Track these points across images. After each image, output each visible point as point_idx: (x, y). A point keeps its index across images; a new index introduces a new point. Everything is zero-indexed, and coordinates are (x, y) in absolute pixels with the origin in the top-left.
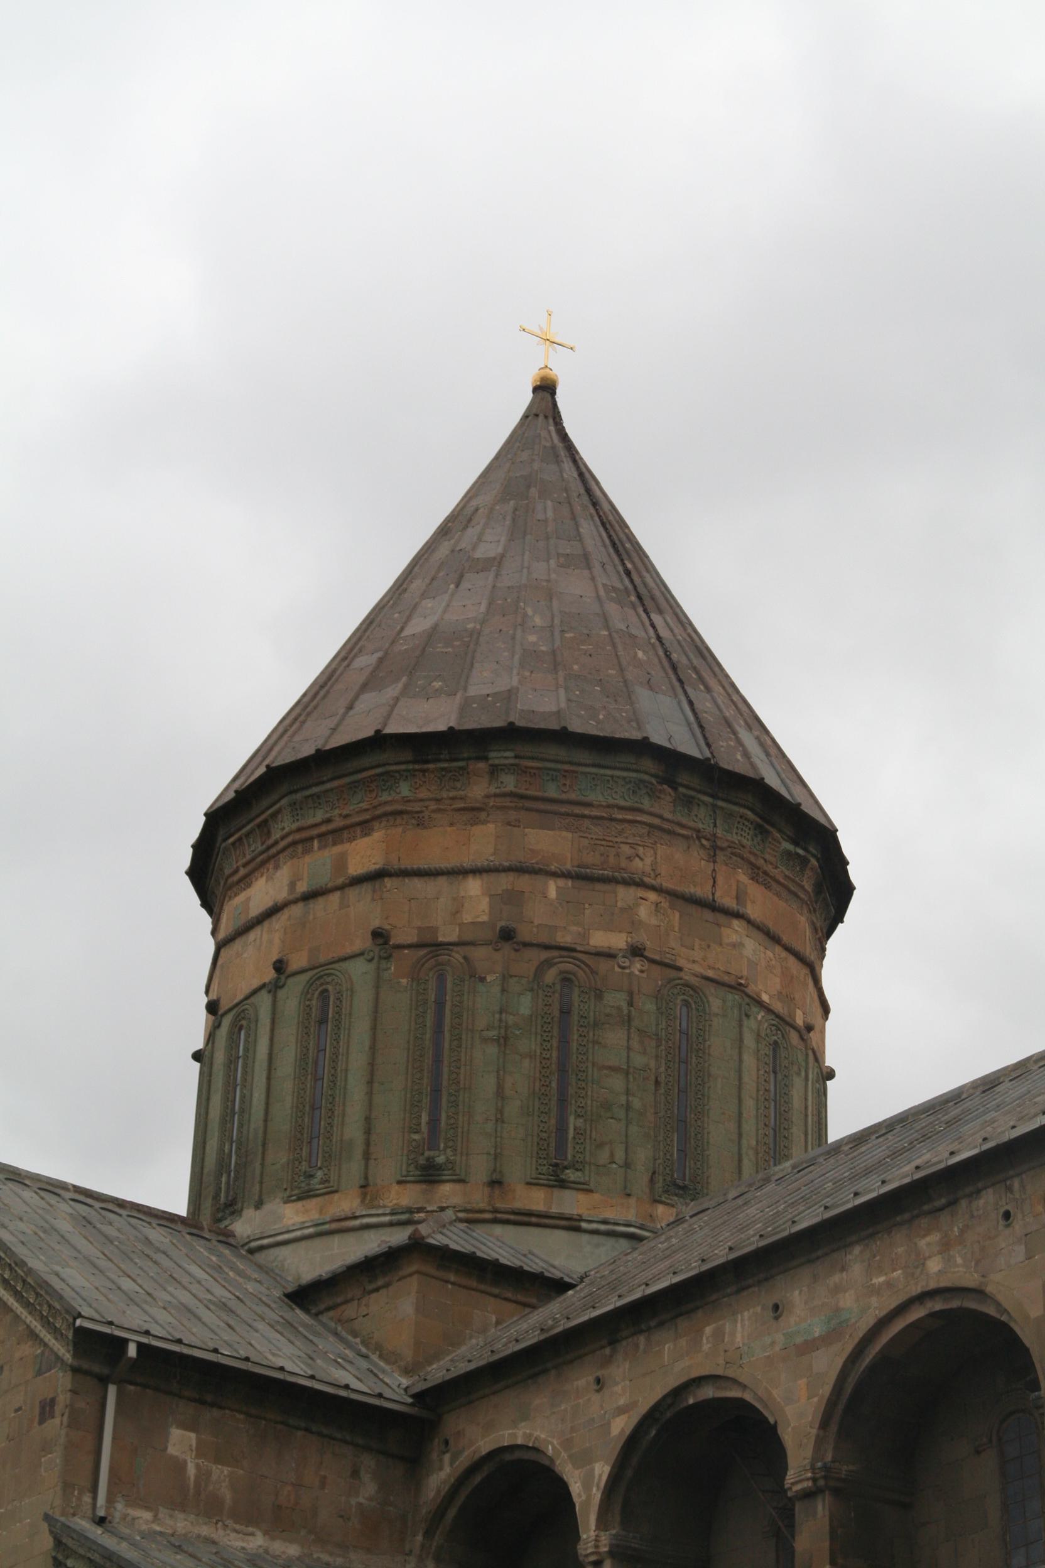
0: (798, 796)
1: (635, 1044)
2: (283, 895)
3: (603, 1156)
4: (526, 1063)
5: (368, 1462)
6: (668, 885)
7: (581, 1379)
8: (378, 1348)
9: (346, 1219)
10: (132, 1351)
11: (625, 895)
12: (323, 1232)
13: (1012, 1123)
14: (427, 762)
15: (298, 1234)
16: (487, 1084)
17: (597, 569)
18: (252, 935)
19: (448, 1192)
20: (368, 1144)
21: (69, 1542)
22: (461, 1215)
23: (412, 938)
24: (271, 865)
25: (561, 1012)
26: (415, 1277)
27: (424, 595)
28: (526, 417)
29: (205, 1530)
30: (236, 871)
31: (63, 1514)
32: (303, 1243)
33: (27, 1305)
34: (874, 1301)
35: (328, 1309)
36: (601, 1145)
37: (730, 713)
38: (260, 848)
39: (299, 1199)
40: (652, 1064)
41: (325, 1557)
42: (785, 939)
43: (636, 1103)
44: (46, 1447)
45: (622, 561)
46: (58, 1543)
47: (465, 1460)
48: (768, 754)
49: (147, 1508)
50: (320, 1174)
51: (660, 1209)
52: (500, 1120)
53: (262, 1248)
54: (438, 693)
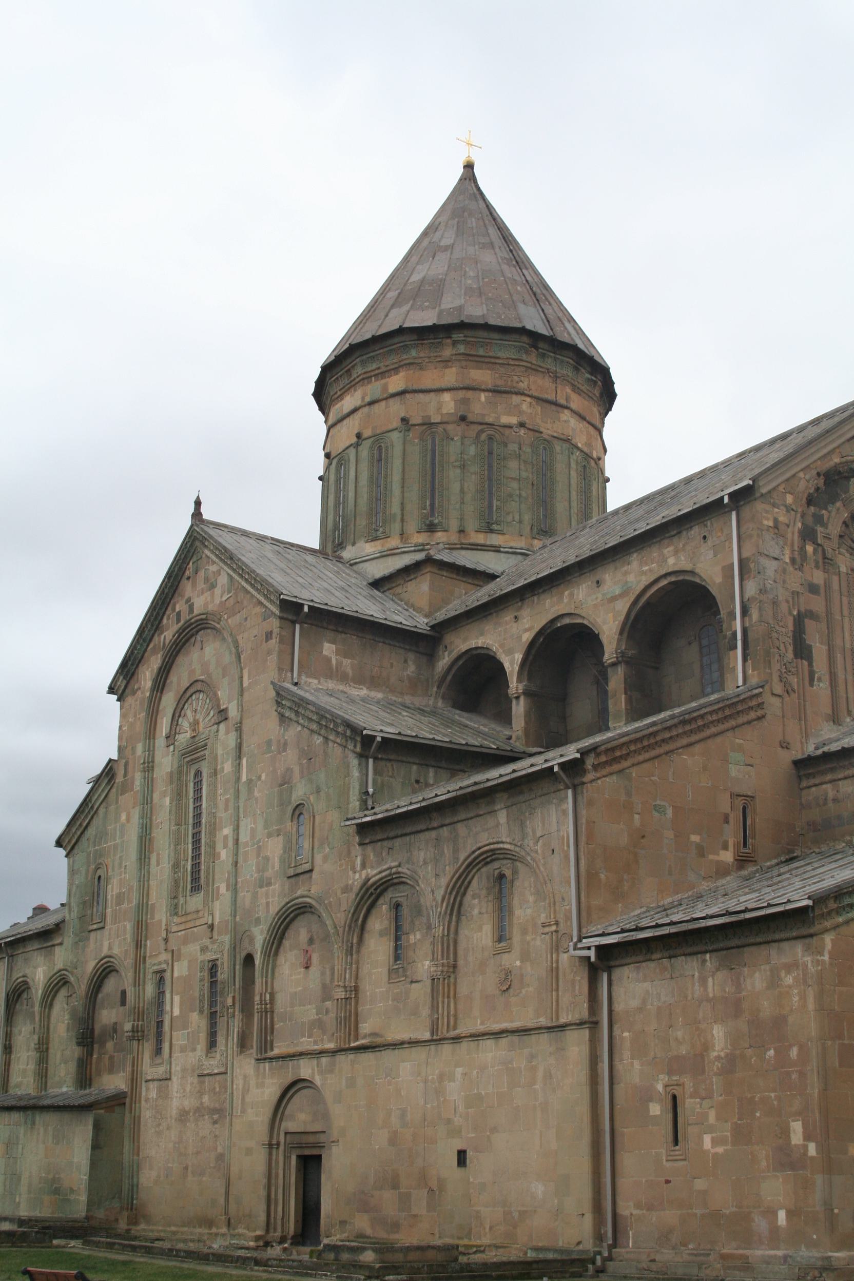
0: (593, 353)
1: (522, 467)
2: (358, 403)
3: (510, 518)
4: (473, 476)
5: (411, 656)
7: (508, 617)
8: (413, 606)
9: (394, 549)
10: (306, 609)
11: (516, 399)
12: (385, 555)
13: (706, 496)
14: (424, 340)
15: (372, 556)
16: (456, 487)
17: (497, 250)
18: (345, 422)
19: (440, 536)
20: (403, 515)
21: (283, 693)
22: (446, 546)
23: (420, 421)
24: (352, 390)
25: (489, 453)
26: (428, 574)
27: (417, 264)
28: (460, 180)
29: (341, 687)
30: (336, 393)
31: (279, 681)
32: (375, 561)
33: (257, 590)
34: (644, 578)
35: (389, 589)
36: (508, 513)
37: (560, 315)
38: (347, 382)
39: (372, 541)
40: (530, 476)
41: (394, 698)
42: (587, 418)
43: (524, 494)
44: (269, 653)
45: (508, 246)
46: (278, 694)
47: (454, 655)
48: (578, 334)
49: (316, 678)
50: (381, 529)
51: (536, 541)
52: (462, 503)
53: (356, 563)
54: (427, 307)
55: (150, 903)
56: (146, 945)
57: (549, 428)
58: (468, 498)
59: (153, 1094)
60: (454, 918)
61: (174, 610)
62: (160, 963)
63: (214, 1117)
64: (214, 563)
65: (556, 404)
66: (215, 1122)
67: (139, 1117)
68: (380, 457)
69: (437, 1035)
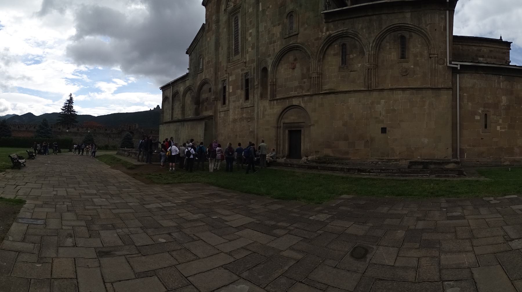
55: (219, 62)
56: (218, 74)
59: (222, 115)
60: (378, 49)
62: (224, 78)
63: (248, 120)
66: (249, 122)
67: (217, 122)
69: (371, 88)
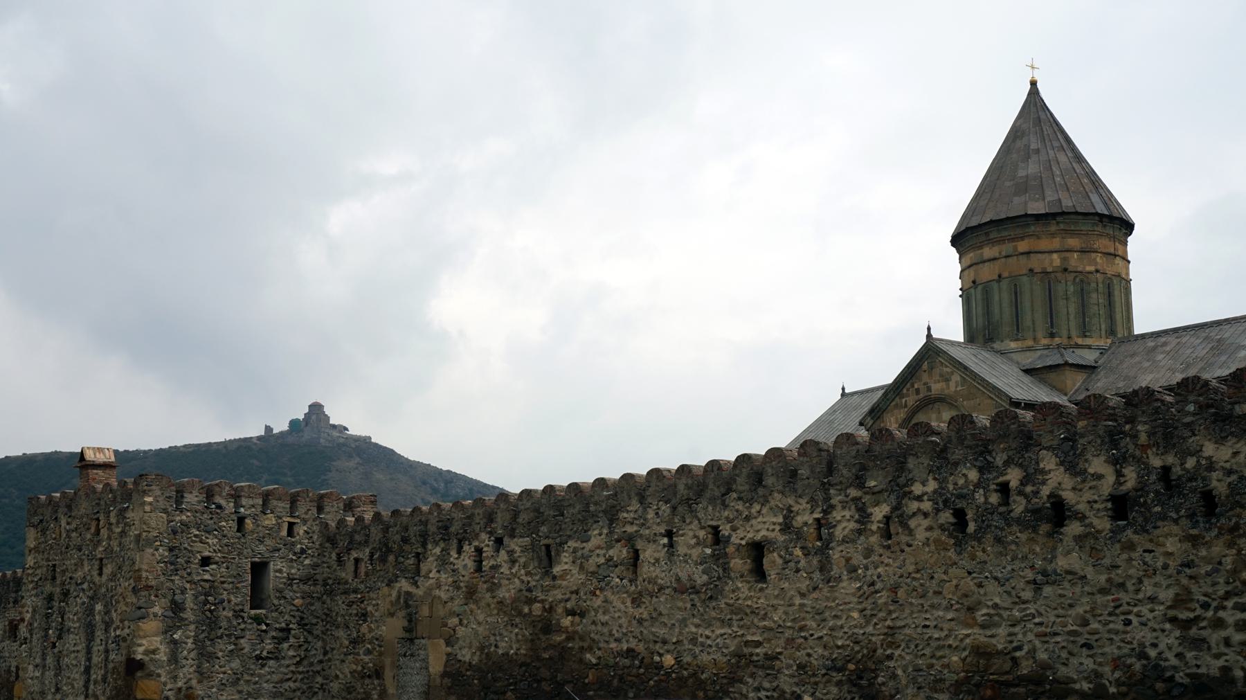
6: (1104, 251)
11: (1093, 255)
18: (986, 264)
19: (1057, 340)
23: (1039, 270)
24: (990, 245)
57: (1110, 271)
58: (1072, 317)
61: (913, 386)
64: (947, 367)
65: (1116, 256)
68: (1016, 293)
